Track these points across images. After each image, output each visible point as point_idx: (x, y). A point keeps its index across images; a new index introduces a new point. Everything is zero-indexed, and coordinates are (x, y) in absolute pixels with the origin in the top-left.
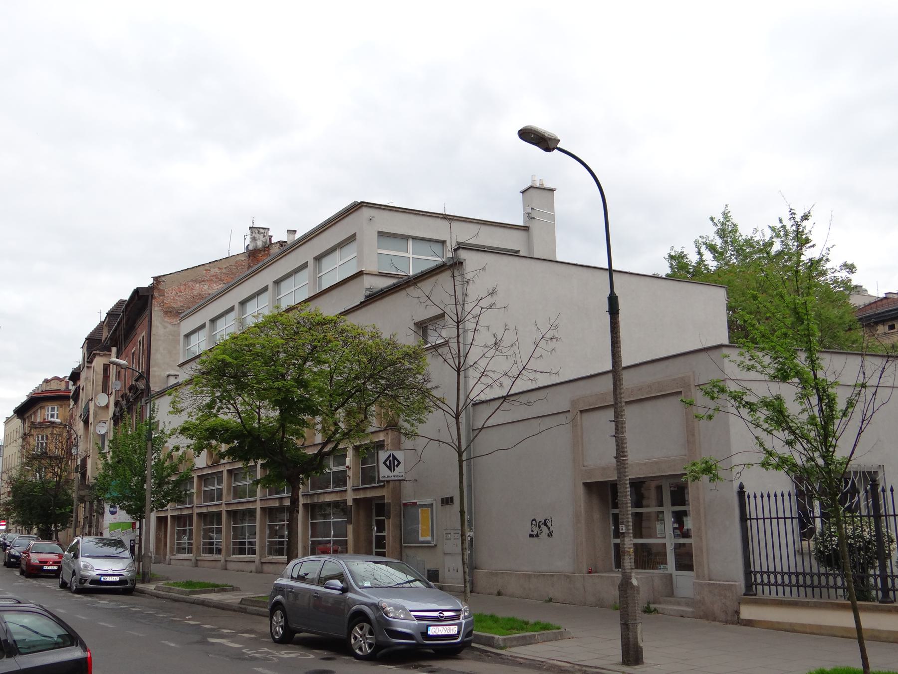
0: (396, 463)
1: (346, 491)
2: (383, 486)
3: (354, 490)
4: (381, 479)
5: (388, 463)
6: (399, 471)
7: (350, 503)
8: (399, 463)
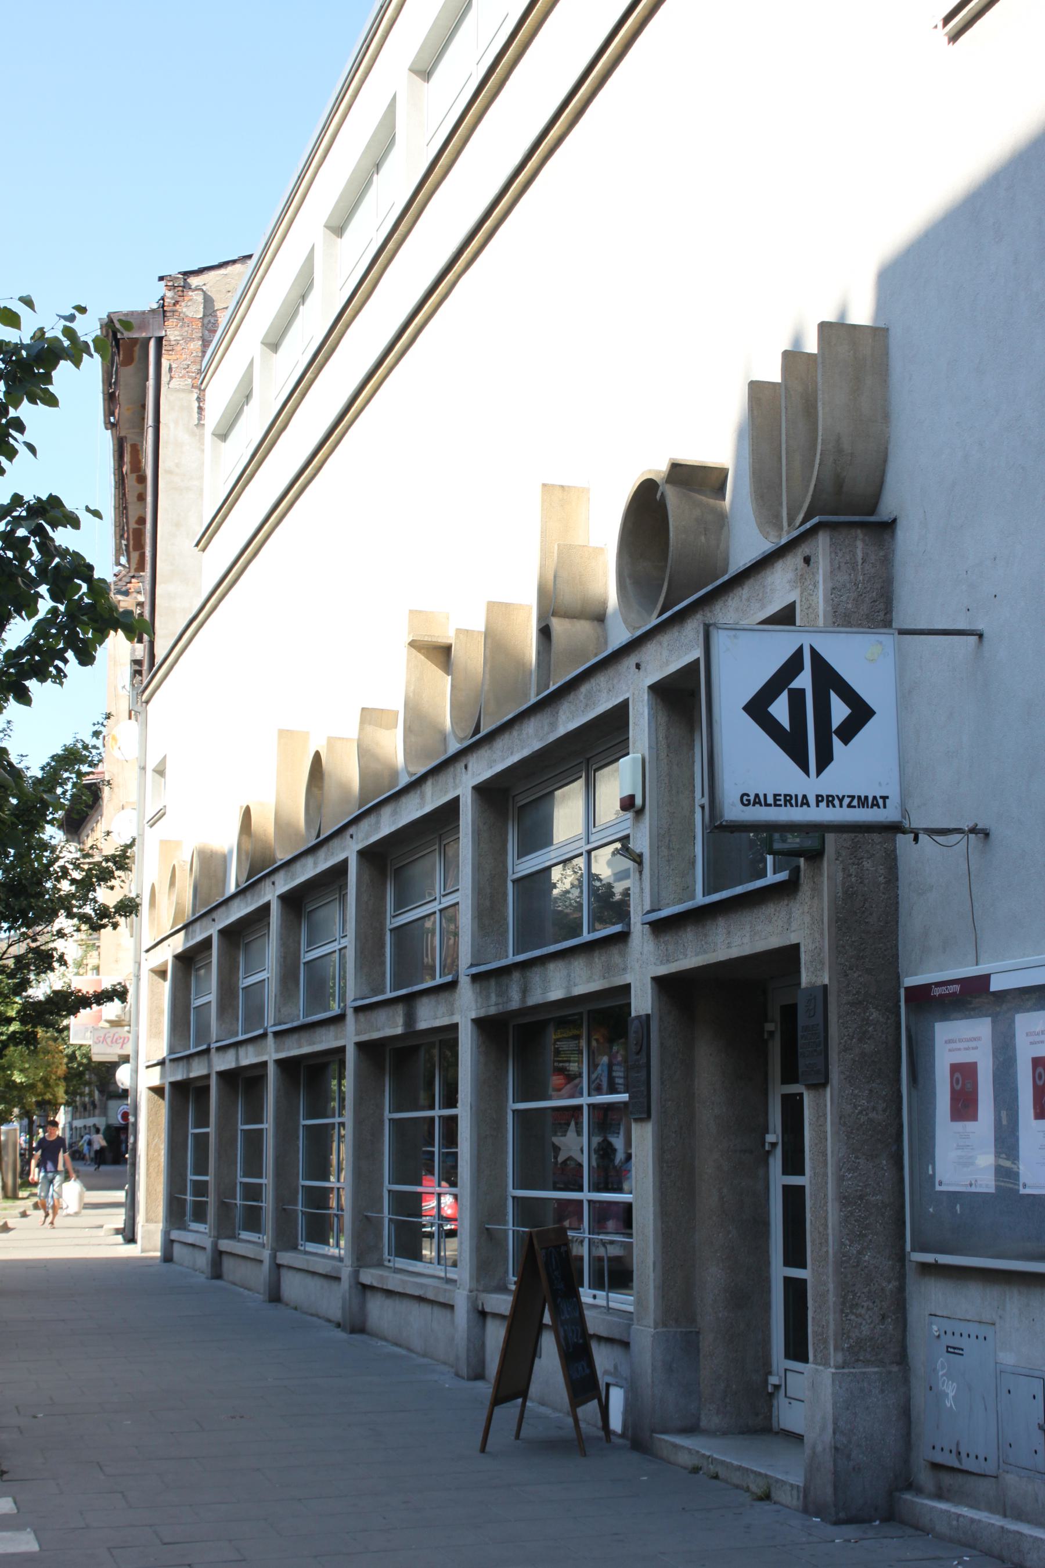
0: (840, 711)
1: (623, 937)
2: (787, 890)
3: (661, 927)
4: (734, 811)
5: (780, 709)
6: (861, 768)
8: (862, 712)
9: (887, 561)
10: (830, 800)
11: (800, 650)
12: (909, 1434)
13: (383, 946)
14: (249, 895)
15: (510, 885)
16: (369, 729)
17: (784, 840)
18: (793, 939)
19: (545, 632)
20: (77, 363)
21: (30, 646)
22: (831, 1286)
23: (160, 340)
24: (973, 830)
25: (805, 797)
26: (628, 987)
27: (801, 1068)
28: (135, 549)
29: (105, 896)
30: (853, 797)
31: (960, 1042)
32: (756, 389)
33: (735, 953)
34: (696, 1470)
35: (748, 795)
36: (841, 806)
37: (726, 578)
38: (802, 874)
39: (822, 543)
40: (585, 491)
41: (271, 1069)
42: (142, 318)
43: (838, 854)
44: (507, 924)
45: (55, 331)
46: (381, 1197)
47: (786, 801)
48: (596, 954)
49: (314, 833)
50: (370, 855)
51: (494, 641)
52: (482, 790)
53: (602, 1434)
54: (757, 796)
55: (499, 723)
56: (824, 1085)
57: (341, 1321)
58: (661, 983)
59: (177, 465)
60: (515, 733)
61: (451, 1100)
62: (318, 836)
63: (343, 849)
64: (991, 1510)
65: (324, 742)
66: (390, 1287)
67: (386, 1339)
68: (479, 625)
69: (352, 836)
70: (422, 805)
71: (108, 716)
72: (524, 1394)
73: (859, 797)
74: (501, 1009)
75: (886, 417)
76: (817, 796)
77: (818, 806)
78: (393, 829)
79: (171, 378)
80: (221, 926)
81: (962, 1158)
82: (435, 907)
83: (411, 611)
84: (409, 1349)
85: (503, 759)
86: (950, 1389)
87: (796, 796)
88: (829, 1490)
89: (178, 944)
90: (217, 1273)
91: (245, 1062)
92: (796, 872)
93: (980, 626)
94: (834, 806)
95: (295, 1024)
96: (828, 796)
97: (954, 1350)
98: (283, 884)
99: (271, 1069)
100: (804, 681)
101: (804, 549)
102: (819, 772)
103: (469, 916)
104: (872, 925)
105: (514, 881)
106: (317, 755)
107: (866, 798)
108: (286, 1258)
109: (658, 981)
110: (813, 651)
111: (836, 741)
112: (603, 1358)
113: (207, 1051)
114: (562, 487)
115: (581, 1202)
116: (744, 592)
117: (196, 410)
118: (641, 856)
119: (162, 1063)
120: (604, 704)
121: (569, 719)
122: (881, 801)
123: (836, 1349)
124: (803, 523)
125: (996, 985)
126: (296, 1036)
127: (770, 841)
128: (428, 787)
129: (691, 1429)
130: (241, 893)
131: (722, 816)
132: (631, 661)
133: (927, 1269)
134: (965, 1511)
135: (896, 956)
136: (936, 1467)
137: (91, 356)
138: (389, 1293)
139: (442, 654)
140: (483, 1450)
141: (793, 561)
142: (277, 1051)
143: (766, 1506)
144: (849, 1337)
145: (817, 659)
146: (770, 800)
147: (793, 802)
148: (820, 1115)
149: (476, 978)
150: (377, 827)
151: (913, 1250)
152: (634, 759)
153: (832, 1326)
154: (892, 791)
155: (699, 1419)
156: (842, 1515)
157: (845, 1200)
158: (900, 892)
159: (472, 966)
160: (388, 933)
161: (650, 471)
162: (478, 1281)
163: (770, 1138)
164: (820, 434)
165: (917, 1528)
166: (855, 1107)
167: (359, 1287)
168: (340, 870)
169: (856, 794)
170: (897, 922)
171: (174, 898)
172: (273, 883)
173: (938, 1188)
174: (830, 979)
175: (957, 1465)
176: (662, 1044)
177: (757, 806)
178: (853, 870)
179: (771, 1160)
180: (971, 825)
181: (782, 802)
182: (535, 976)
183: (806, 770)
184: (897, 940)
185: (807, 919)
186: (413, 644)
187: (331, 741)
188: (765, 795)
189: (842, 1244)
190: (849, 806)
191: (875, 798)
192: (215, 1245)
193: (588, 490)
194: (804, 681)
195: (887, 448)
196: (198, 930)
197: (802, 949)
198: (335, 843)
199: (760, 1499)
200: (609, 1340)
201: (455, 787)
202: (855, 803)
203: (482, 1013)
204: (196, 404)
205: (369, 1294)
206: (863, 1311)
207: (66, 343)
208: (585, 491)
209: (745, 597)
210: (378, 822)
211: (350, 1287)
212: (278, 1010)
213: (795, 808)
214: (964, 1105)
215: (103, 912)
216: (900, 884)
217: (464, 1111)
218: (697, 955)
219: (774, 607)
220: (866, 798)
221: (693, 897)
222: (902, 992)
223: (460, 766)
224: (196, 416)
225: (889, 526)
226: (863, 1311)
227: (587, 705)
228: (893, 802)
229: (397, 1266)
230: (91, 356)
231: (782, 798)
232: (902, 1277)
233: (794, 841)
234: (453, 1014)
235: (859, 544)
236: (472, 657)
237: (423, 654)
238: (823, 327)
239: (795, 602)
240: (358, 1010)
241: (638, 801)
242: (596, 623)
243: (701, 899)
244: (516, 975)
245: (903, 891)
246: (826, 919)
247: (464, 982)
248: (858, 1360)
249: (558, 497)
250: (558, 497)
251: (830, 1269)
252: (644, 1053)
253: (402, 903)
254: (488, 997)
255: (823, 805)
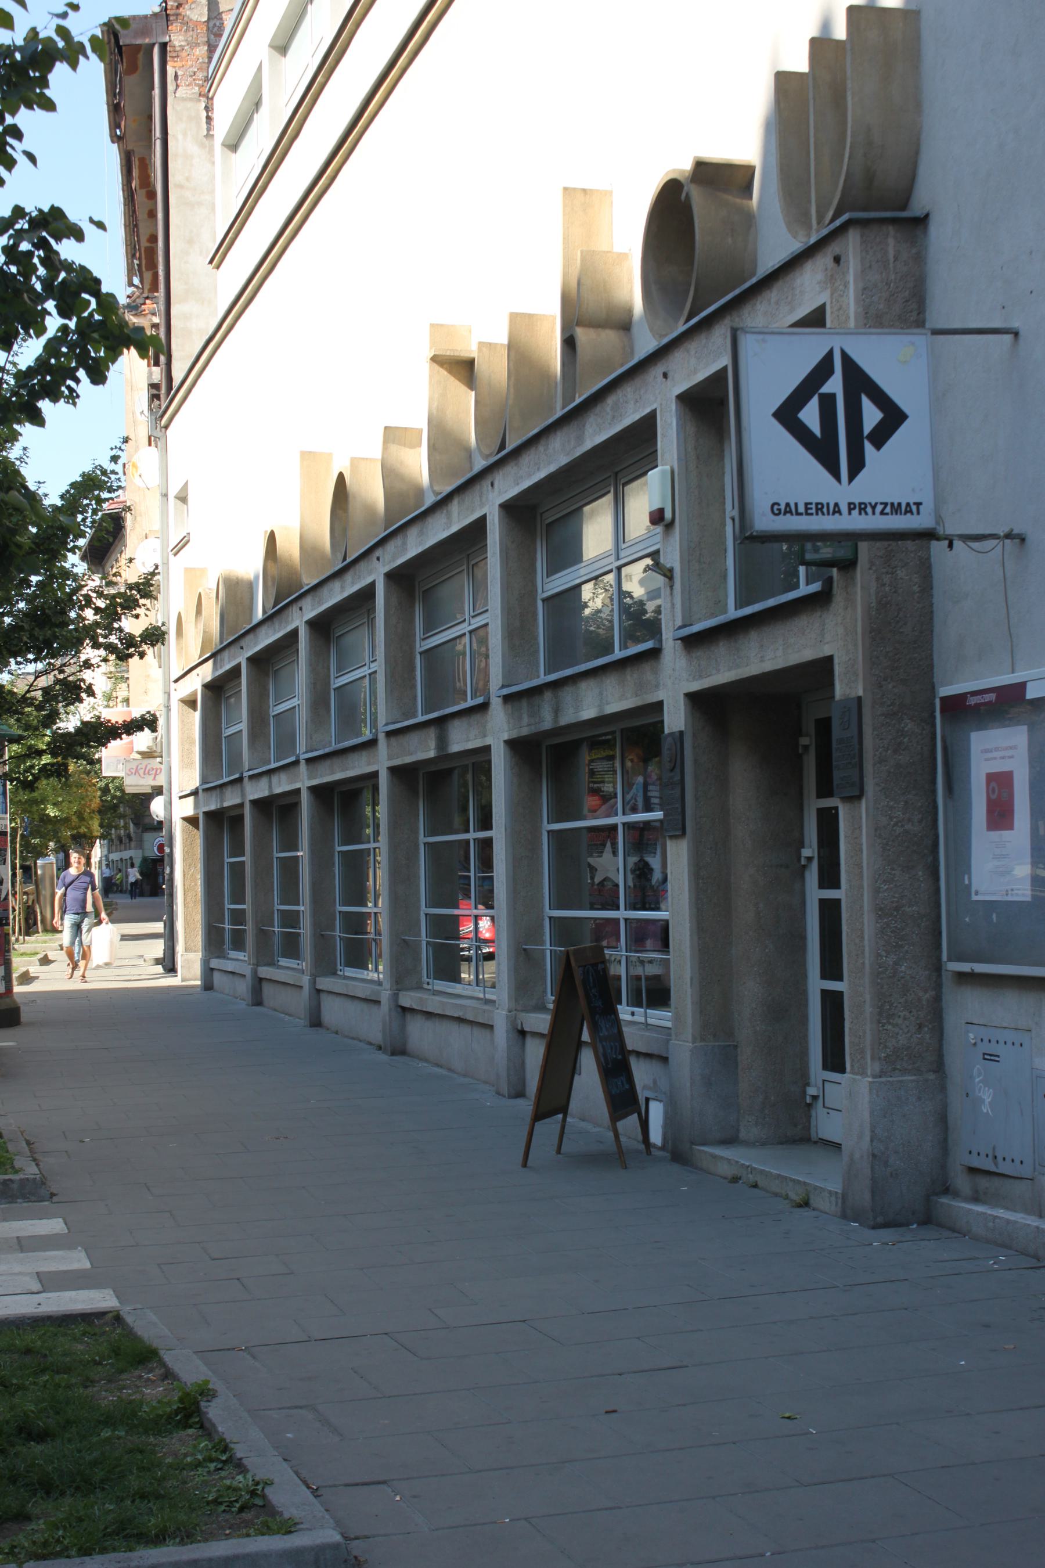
0: (871, 416)
1: (654, 654)
2: (821, 600)
3: (693, 642)
4: (764, 522)
5: (810, 415)
6: (894, 474)
7: (675, 719)
8: (894, 417)
9: (920, 259)
10: (862, 508)
11: (830, 353)
12: (946, 1140)
13: (412, 669)
14: (276, 621)
15: (540, 604)
16: (393, 448)
17: (816, 550)
18: (826, 651)
19: (569, 343)
20: (74, 65)
21: (41, 365)
22: (868, 997)
23: (164, 46)
24: (1009, 536)
25: (836, 505)
26: (660, 705)
27: (836, 781)
28: (147, 269)
29: (132, 625)
30: (886, 504)
31: (996, 751)
32: (783, 80)
33: (768, 666)
34: (735, 1180)
35: (779, 504)
36: (874, 513)
37: (754, 280)
38: (835, 585)
39: (852, 240)
40: (609, 193)
41: (305, 796)
42: (145, 23)
43: (872, 563)
44: (538, 644)
45: (47, 31)
46: (419, 921)
47: (817, 509)
48: (628, 671)
49: (340, 557)
50: (398, 577)
51: (519, 354)
52: (511, 509)
53: (642, 1147)
54: (788, 505)
55: (524, 438)
56: (859, 797)
57: (382, 1043)
58: (696, 700)
59: (188, 179)
60: (541, 448)
61: (486, 822)
62: (345, 559)
63: (370, 573)
64: (1027, 1211)
65: (348, 464)
66: (429, 1010)
67: (426, 1061)
68: (502, 338)
69: (378, 559)
70: (449, 525)
71: (126, 440)
72: (564, 1110)
73: (892, 504)
74: (533, 729)
75: (918, 106)
76: (850, 504)
77: (850, 513)
78: (420, 550)
79: (177, 86)
80: (250, 654)
81: (997, 868)
82: (465, 628)
83: (432, 325)
84: (450, 1070)
85: (530, 475)
86: (987, 1096)
87: (828, 504)
88: (867, 1196)
89: (207, 673)
90: (258, 1001)
91: (278, 790)
92: (829, 582)
93: (1015, 324)
94: (866, 514)
95: (327, 750)
96: (860, 504)
97: (990, 1057)
98: (311, 609)
99: (305, 796)
100: (835, 385)
101: (834, 248)
102: (852, 477)
103: (499, 636)
104: (906, 635)
105: (543, 600)
106: (341, 476)
107: (899, 504)
108: (325, 983)
109: (693, 698)
110: (845, 356)
111: (868, 447)
112: (642, 1073)
113: (240, 780)
114: (584, 191)
115: (616, 921)
116: (773, 294)
117: (204, 120)
118: (671, 570)
119: (195, 793)
120: (632, 416)
121: (597, 432)
122: (914, 508)
123: (873, 1058)
124: (832, 221)
125: (1032, 693)
126: (327, 763)
127: (803, 551)
128: (455, 506)
129: (730, 1140)
130: (268, 619)
131: (752, 527)
132: (657, 371)
133: (964, 978)
134: (1001, 1213)
135: (931, 666)
136: (973, 1171)
137: (87, 58)
138: (429, 1015)
139: (464, 369)
140: (525, 1164)
141: (823, 261)
142: (310, 778)
143: (804, 1212)
144: (886, 1047)
145: (848, 362)
146: (801, 509)
147: (825, 510)
148: (855, 827)
149: (507, 699)
150: (404, 549)
151: (950, 960)
152: (663, 472)
153: (868, 1038)
154: (927, 498)
155: (738, 1130)
156: (880, 1220)
157: (881, 912)
158: (934, 601)
159: (503, 687)
160: (418, 656)
161: (674, 170)
162: (516, 1000)
163: (806, 852)
164: (849, 125)
165: (953, 1230)
166: (891, 818)
167: (399, 1009)
168: (367, 594)
169: (889, 501)
170: (932, 631)
171: (201, 626)
172: (301, 609)
173: (974, 898)
174: (864, 690)
175: (993, 1169)
176: (696, 761)
177: (788, 515)
178: (887, 579)
179: (807, 874)
180: (1007, 530)
181: (813, 511)
182: (567, 694)
183: (837, 476)
184: (931, 650)
185: (841, 630)
186: (435, 359)
187: (355, 462)
188: (796, 504)
189: (879, 955)
190: (882, 513)
191: (908, 504)
192: (255, 972)
193: (611, 192)
194: (835, 385)
195: (919, 139)
196: (226, 658)
197: (836, 661)
198: (362, 565)
199: (800, 1206)
200: (648, 1056)
201: (482, 505)
202: (888, 510)
203: (515, 734)
204: (205, 114)
205: (409, 1016)
206: (900, 1021)
207: (61, 44)
208: (609, 193)
209: (773, 300)
210: (404, 544)
211: (390, 1010)
212: (309, 737)
213: (826, 516)
214: (1000, 815)
215: (130, 641)
216: (935, 591)
217: (499, 833)
218: (729, 670)
219: (803, 311)
220: (899, 504)
221: (725, 612)
222: (938, 702)
223: (486, 484)
224: (205, 126)
225: (921, 222)
226: (900, 1021)
227: (614, 417)
228: (927, 508)
229: (436, 988)
230: (87, 58)
231: (813, 506)
232: (938, 986)
233: (826, 552)
234: (485, 736)
235: (891, 241)
236: (495, 370)
237: (446, 369)
238: (852, 10)
239: (824, 305)
240: (389, 734)
241: (668, 515)
242: (621, 332)
243: (733, 613)
244: (548, 695)
245: (938, 599)
246: (859, 630)
247: (496, 703)
248: (894, 1069)
249: (580, 202)
250: (580, 202)
251: (867, 980)
252: (678, 770)
253: (431, 625)
254: (520, 718)
255: (855, 512)
